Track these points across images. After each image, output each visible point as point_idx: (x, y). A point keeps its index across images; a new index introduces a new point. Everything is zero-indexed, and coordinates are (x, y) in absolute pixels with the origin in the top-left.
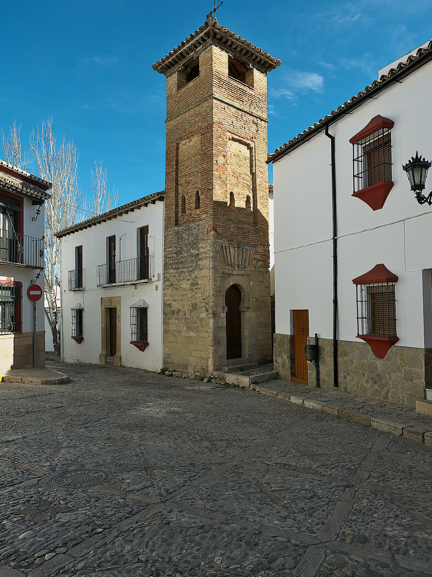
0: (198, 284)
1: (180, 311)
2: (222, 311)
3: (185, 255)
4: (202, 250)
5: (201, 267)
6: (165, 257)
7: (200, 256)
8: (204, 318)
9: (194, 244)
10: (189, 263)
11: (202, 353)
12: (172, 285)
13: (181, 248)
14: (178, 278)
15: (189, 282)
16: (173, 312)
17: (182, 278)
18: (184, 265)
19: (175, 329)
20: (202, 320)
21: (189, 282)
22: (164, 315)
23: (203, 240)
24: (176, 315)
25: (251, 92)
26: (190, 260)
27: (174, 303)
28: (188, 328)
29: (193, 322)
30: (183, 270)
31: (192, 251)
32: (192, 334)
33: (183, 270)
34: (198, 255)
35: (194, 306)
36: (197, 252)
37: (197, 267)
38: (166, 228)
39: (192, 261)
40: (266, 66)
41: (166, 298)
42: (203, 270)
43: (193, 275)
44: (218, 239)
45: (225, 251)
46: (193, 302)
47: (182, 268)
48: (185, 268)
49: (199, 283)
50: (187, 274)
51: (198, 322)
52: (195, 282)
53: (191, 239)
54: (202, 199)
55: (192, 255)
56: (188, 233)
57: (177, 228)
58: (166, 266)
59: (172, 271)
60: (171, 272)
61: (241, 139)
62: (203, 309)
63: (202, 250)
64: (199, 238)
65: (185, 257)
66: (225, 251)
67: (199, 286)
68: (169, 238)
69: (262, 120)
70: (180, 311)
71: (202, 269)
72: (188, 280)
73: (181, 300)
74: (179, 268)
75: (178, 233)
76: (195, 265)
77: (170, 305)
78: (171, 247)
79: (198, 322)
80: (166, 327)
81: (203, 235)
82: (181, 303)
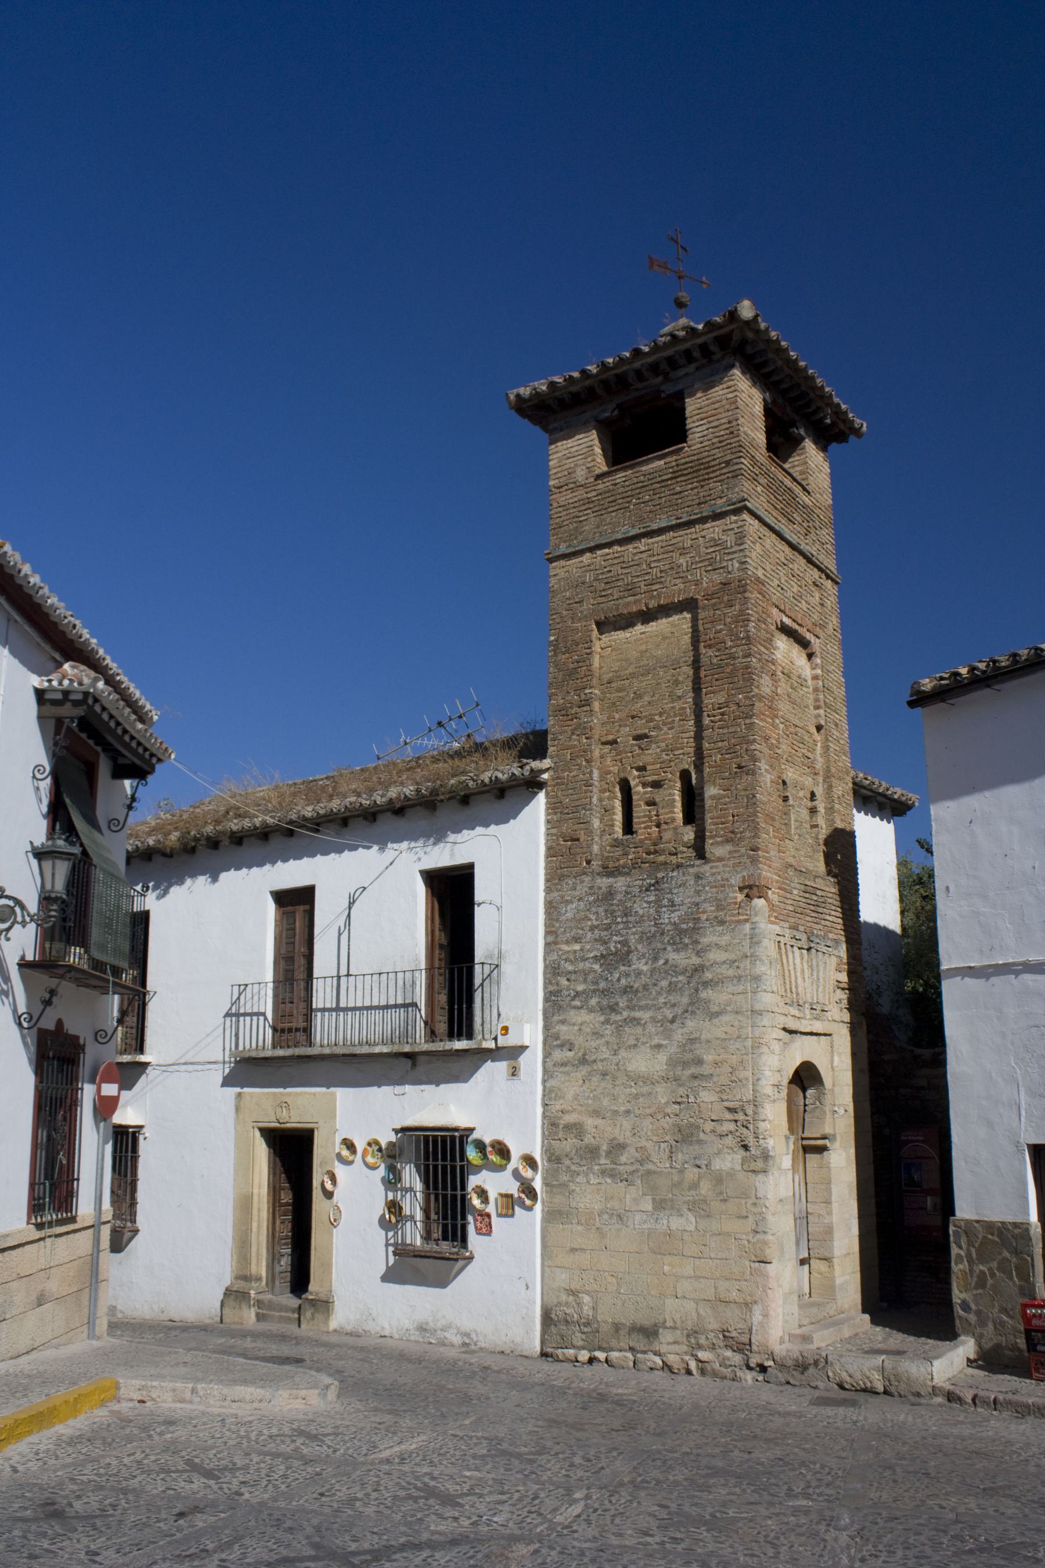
0: (699, 1062)
1: (622, 1147)
2: (784, 1151)
3: (645, 968)
4: (714, 956)
5: (715, 1008)
6: (552, 971)
7: (708, 975)
8: (731, 1174)
9: (687, 934)
10: (659, 993)
11: (723, 1285)
12: (583, 1061)
13: (625, 943)
14: (613, 1040)
15: (662, 1057)
16: (593, 1152)
17: (632, 1042)
18: (639, 999)
19: (597, 1207)
20: (719, 1179)
21: (662, 1057)
22: (549, 1160)
23: (722, 923)
24: (603, 1161)
25: (806, 499)
26: (664, 983)
27: (590, 1122)
28: (660, 1205)
29: (680, 1183)
30: (637, 1014)
31: (672, 956)
32: (676, 1223)
33: (637, 1014)
34: (698, 969)
35: (686, 1136)
36: (695, 960)
37: (696, 1006)
38: (555, 878)
39: (672, 988)
40: (832, 433)
41: (557, 1106)
42: (725, 1018)
43: (680, 1031)
44: (772, 923)
45: (785, 961)
46: (686, 1119)
47: (631, 1008)
48: (646, 1008)
49: (709, 1058)
50: (651, 1028)
51: (705, 1188)
52: (689, 1056)
53: (667, 917)
54: (713, 797)
55: (674, 970)
56: (652, 898)
57: (604, 882)
58: (554, 1002)
59: (583, 1016)
60: (579, 1020)
61: (797, 627)
62: (729, 1141)
63: (714, 956)
64: (704, 917)
65: (639, 973)
66: (784, 957)
67: (706, 1069)
68: (569, 912)
69: (828, 577)
70: (622, 1147)
71: (718, 1014)
72: (659, 1046)
73: (628, 1112)
74: (613, 1009)
75: (610, 894)
76: (685, 1000)
77: (576, 1129)
78: (577, 940)
79: (705, 1188)
80: (559, 1199)
81: (719, 907)
82: (627, 1124)
